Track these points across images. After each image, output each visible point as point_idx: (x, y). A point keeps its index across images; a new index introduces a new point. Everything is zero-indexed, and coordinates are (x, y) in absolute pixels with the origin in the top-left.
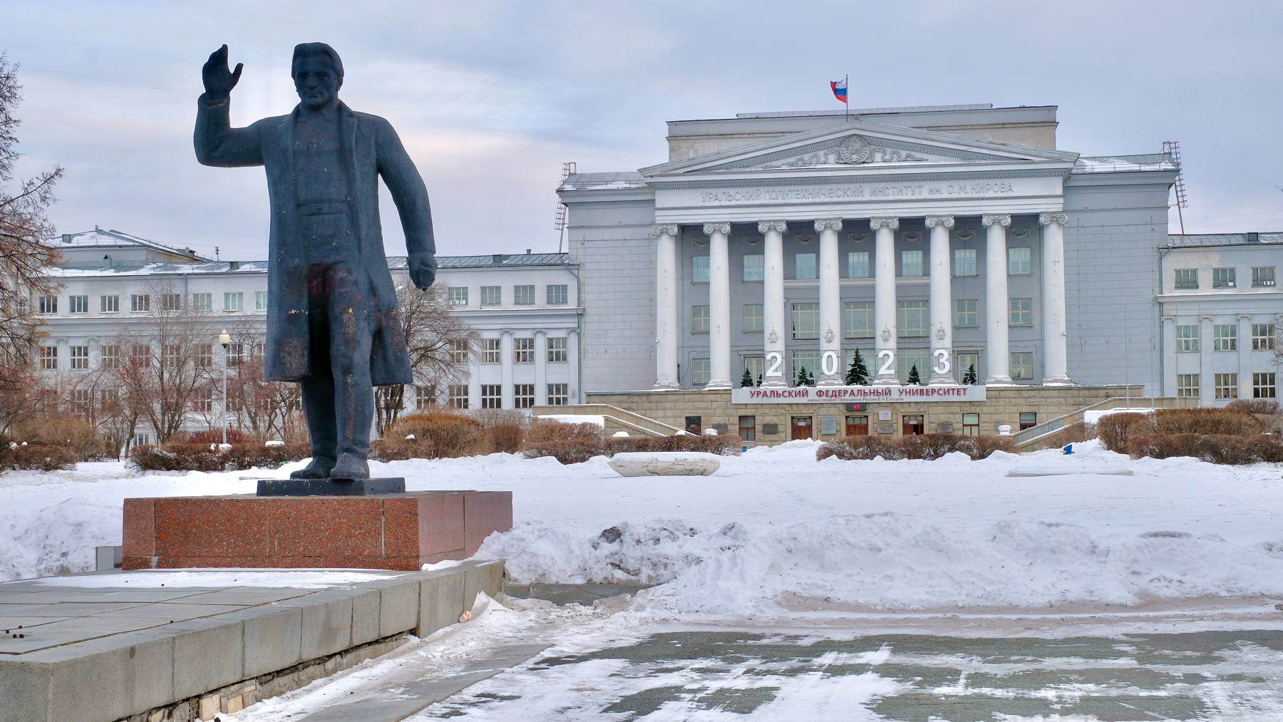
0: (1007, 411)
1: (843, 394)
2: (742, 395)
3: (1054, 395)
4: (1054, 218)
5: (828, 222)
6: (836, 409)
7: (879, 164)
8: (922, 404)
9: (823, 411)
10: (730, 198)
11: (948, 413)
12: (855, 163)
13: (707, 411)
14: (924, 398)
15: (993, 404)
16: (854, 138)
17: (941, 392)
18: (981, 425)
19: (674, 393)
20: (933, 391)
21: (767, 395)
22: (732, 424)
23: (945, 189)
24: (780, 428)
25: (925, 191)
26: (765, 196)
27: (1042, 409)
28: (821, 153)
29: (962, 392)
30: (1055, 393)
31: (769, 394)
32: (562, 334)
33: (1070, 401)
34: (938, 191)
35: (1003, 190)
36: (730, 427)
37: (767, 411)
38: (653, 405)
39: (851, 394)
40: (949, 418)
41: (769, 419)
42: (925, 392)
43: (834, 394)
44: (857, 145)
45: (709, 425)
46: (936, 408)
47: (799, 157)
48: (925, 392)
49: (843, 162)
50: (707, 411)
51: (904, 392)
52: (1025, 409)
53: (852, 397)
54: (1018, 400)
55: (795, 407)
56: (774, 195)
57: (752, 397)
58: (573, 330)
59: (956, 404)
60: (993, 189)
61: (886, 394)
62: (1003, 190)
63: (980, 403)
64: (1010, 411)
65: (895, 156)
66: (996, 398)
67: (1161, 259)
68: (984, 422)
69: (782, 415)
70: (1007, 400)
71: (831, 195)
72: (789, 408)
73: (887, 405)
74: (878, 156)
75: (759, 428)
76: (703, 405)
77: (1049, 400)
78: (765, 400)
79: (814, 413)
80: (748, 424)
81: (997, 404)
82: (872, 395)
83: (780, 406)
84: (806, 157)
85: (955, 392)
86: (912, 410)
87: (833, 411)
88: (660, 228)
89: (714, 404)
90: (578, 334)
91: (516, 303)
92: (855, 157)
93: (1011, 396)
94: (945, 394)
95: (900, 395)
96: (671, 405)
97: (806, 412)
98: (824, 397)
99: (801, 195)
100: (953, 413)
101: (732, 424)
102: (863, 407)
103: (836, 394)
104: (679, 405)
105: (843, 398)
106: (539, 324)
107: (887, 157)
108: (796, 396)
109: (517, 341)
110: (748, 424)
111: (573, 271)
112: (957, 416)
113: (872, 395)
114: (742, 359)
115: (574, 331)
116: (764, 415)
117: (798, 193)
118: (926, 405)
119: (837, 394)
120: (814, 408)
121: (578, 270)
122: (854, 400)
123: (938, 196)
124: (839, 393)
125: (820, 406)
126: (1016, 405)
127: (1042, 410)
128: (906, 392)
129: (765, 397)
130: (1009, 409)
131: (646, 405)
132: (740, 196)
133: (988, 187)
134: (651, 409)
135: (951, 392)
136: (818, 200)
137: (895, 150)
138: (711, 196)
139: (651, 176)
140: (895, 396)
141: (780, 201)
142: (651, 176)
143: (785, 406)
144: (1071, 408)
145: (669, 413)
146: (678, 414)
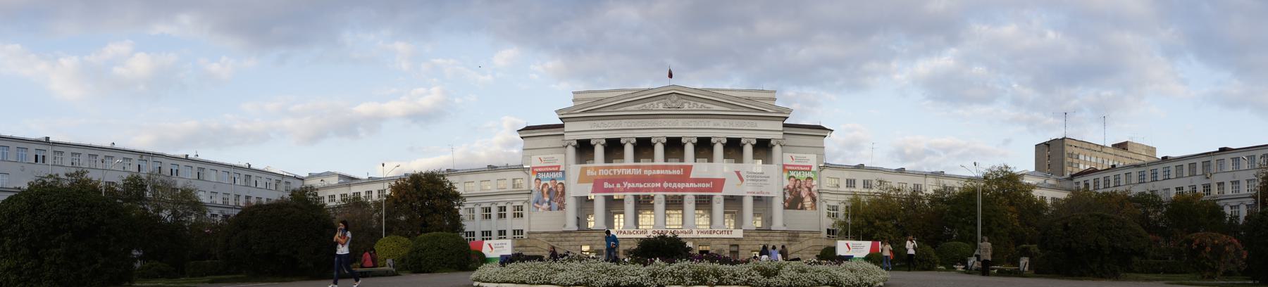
12: (674, 107)
18: (740, 251)
19: (574, 232)
20: (714, 232)
23: (722, 123)
25: (711, 123)
26: (624, 124)
28: (655, 103)
30: (778, 234)
32: (520, 204)
34: (718, 124)
37: (626, 242)
44: (675, 97)
54: (758, 238)
56: (629, 124)
58: (526, 201)
60: (747, 124)
74: (686, 107)
76: (590, 238)
84: (647, 104)
88: (567, 142)
89: (596, 238)
92: (674, 105)
106: (509, 198)
107: (691, 106)
123: (718, 127)
126: (757, 240)
141: (633, 127)
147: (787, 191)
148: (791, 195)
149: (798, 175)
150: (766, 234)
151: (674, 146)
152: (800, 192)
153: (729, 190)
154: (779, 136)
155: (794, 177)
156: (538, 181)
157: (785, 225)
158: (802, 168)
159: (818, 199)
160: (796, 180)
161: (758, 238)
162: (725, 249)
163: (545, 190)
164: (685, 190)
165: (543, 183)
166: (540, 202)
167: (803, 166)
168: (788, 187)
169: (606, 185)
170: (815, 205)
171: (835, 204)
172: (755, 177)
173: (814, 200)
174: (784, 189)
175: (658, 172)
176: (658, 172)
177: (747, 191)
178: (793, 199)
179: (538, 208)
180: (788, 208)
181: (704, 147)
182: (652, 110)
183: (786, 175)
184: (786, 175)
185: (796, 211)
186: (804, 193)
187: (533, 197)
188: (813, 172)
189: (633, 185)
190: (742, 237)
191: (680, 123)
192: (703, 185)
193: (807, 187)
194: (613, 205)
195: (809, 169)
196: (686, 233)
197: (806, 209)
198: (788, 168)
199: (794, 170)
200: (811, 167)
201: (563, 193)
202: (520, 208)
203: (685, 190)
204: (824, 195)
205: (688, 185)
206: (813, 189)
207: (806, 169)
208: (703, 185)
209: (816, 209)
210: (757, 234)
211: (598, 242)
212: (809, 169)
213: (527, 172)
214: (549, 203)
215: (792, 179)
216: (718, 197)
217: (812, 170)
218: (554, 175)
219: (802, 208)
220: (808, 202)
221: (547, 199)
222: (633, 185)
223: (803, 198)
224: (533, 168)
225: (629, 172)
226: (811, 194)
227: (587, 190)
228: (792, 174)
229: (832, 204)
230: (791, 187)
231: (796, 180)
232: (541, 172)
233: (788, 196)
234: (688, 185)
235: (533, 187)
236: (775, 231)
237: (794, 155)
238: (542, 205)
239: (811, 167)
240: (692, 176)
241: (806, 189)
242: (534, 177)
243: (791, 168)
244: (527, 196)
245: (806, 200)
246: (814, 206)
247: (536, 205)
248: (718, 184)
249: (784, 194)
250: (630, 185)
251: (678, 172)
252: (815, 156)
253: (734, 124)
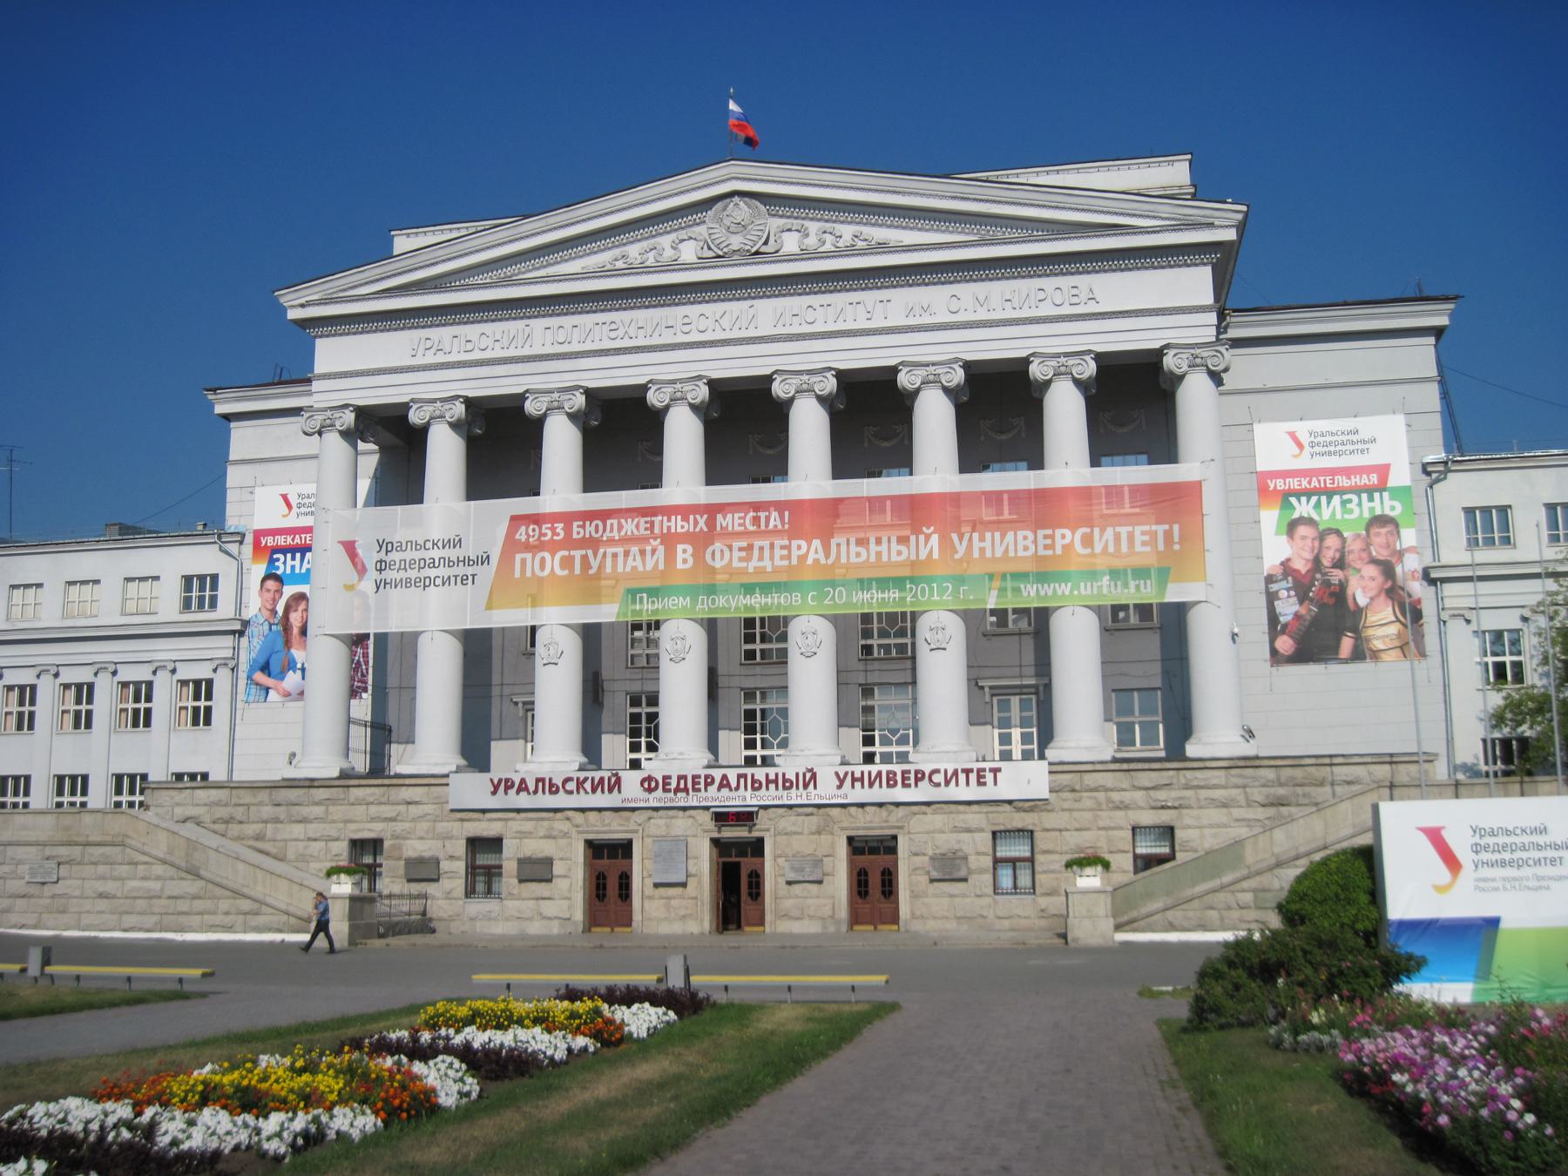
0: (1101, 824)
1: (702, 786)
2: (472, 790)
3: (1214, 781)
5: (678, 386)
6: (691, 820)
8: (892, 807)
9: (658, 824)
10: (469, 347)
11: (956, 830)
13: (399, 827)
14: (900, 794)
15: (1066, 805)
16: (736, 199)
17: (939, 778)
18: (1039, 858)
21: (526, 789)
22: (452, 857)
24: (558, 868)
25: (898, 304)
26: (541, 333)
27: (1188, 817)
28: (665, 241)
29: (989, 777)
30: (1217, 777)
31: (531, 786)
32: (202, 672)
33: (1258, 794)
35: (1075, 300)
36: (445, 865)
37: (528, 826)
38: (281, 812)
39: (721, 786)
40: (959, 842)
41: (536, 847)
42: (899, 778)
43: (682, 786)
44: (740, 210)
45: (400, 858)
46: (929, 818)
47: (617, 252)
48: (899, 778)
49: (711, 254)
50: (399, 827)
51: (849, 779)
52: (1147, 818)
53: (725, 791)
55: (592, 816)
57: (494, 793)
59: (975, 808)
61: (806, 786)
62: (1075, 300)
63: (1033, 805)
64: (1108, 823)
65: (829, 238)
66: (1073, 790)
67: (1431, 487)
68: (1045, 852)
69: (566, 835)
70: (1101, 796)
71: (686, 328)
72: (579, 817)
73: (810, 810)
75: (510, 866)
76: (388, 811)
77: (1204, 793)
78: (523, 801)
79: (636, 832)
80: (483, 859)
81: (1076, 805)
82: (772, 786)
83: (559, 815)
84: (634, 251)
85: (973, 777)
86: (871, 824)
87: (681, 824)
88: (319, 418)
89: (413, 809)
90: (233, 669)
91: (123, 614)
92: (736, 242)
93: (1109, 784)
94: (947, 783)
95: (840, 787)
96: (318, 811)
97: (613, 829)
98: (659, 793)
99: (620, 333)
100: (969, 830)
101: (452, 857)
102: (745, 818)
103: (687, 784)
104: (337, 812)
105: (703, 794)
106: (164, 650)
108: (594, 790)
109: (125, 685)
110: (483, 859)
111: (230, 547)
112: (977, 835)
113: (772, 786)
114: (521, 713)
115: (226, 664)
116: (522, 835)
117: (613, 326)
118: (901, 811)
119: (690, 785)
120: (637, 817)
121: (241, 542)
122: (728, 798)
123: (927, 320)
124: (694, 783)
125: (650, 813)
127: (1188, 821)
128: (854, 780)
129: (524, 794)
130: (1106, 818)
131: (268, 811)
133: (1041, 295)
134: (277, 820)
135: (962, 777)
136: (656, 341)
137: (828, 225)
138: (429, 344)
139: (302, 306)
140: (826, 790)
141: (576, 347)
142: (302, 306)
143: (570, 814)
144: (1261, 813)
145: (313, 829)
146: (334, 834)
147: (1282, 588)
148: (1302, 599)
149: (1329, 512)
150: (1163, 777)
152: (1343, 586)
154: (1203, 327)
155: (1310, 522)
156: (271, 584)
157: (1250, 734)
158: (1343, 481)
159: (1428, 609)
160: (1322, 536)
161: (1127, 797)
162: (968, 849)
165: (289, 591)
166: (274, 667)
167: (1348, 472)
170: (1419, 637)
171: (1509, 621)
174: (1270, 579)
178: (1316, 621)
179: (267, 689)
180: (1303, 655)
182: (644, 270)
183: (1270, 517)
184: (1270, 517)
185: (1334, 668)
186: (1362, 588)
187: (250, 650)
188: (1402, 493)
190: (1045, 794)
191: (767, 313)
193: (1374, 561)
195: (1374, 479)
196: (788, 784)
197: (1375, 655)
198: (1280, 484)
199: (1308, 493)
200: (1383, 471)
202: (203, 688)
204: (1449, 589)
207: (1364, 480)
209: (1422, 654)
210: (1122, 780)
211: (423, 826)
212: (1374, 479)
213: (233, 548)
215: (1302, 530)
217: (1390, 484)
219: (1358, 655)
220: (1382, 624)
223: (1359, 612)
224: (259, 534)
226: (1393, 591)
228: (1303, 508)
229: (1492, 622)
230: (1301, 566)
231: (1322, 536)
232: (284, 550)
233: (1288, 608)
235: (254, 606)
236: (1203, 764)
237: (1303, 428)
238: (281, 676)
239: (1383, 471)
241: (1372, 571)
242: (260, 569)
243: (1294, 483)
244: (228, 641)
245: (1372, 618)
246: (1412, 640)
247: (260, 677)
249: (1271, 598)
252: (1399, 420)
253: (995, 301)
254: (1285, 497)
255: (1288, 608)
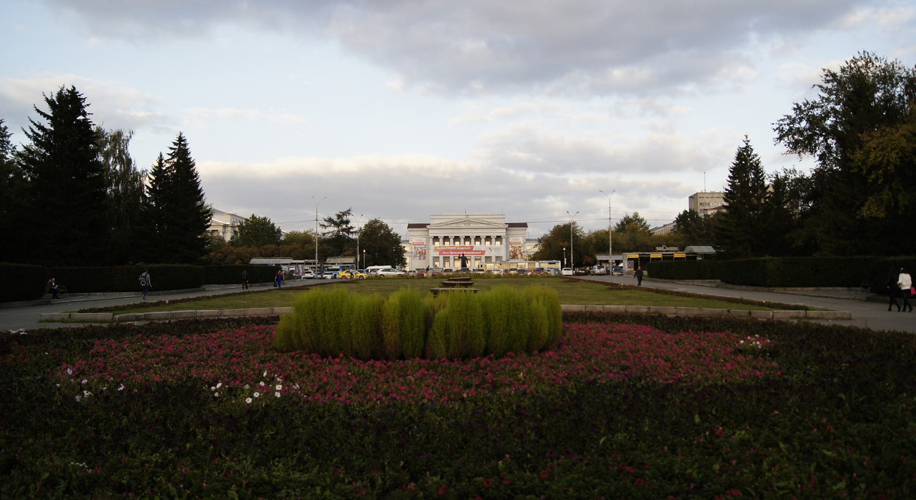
4: (504, 237)
7: (472, 226)
23: (484, 231)
25: (480, 231)
26: (450, 231)
60: (493, 231)
132: (445, 231)
151: (467, 238)
153: (487, 254)
163: (418, 252)
164: (471, 254)
168: (512, 251)
169: (444, 253)
172: (497, 249)
173: (522, 255)
175: (462, 248)
176: (462, 248)
177: (493, 254)
181: (478, 238)
184: (510, 246)
187: (413, 254)
189: (453, 253)
191: (470, 231)
192: (477, 253)
194: (446, 259)
201: (425, 253)
203: (471, 254)
205: (472, 253)
206: (521, 251)
208: (477, 253)
214: (419, 257)
216: (483, 257)
218: (422, 246)
220: (519, 256)
221: (418, 255)
222: (453, 253)
225: (451, 248)
226: (521, 253)
227: (437, 254)
228: (513, 245)
233: (511, 254)
234: (472, 253)
235: (413, 250)
240: (474, 250)
248: (483, 253)
250: (452, 253)
251: (469, 248)
254: (511, 244)
255: (511, 254)
